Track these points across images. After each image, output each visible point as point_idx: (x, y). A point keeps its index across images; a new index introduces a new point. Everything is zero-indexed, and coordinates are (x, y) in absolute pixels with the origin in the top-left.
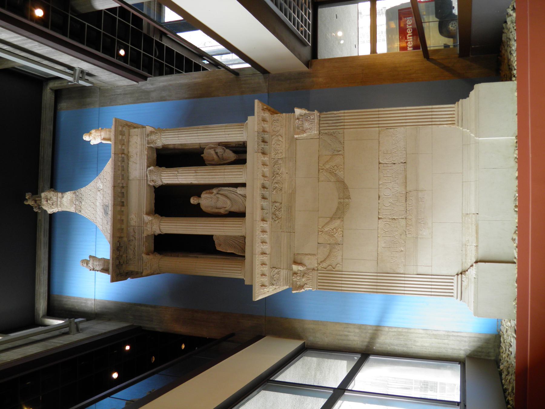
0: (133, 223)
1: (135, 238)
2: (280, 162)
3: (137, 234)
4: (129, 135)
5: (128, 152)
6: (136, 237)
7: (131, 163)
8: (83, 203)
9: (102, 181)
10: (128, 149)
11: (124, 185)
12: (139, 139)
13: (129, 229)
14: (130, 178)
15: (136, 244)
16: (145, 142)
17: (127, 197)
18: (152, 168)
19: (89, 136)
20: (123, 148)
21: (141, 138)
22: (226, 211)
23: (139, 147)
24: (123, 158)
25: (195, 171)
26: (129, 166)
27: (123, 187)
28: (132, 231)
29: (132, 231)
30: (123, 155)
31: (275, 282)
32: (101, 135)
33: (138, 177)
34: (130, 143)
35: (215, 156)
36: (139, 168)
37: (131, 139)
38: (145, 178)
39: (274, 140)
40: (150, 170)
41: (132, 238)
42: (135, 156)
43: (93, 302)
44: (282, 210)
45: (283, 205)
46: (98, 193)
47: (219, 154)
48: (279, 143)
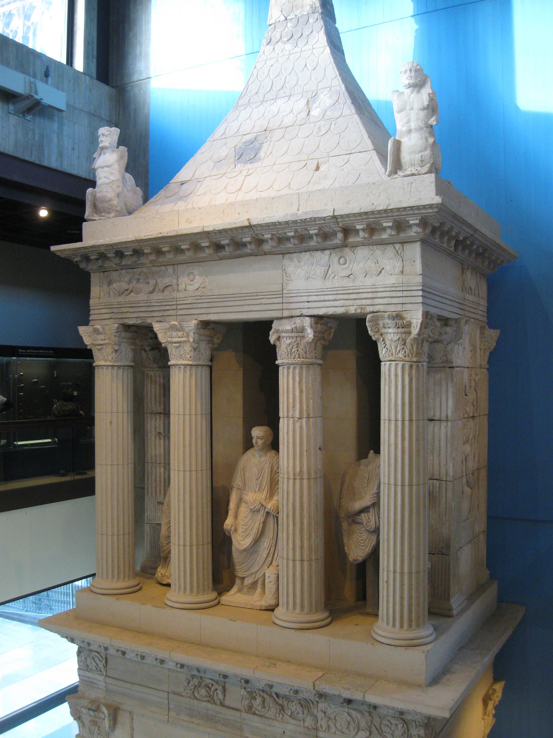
0: (184, 281)
1: (151, 292)
2: (309, 722)
3: (161, 296)
4: (403, 243)
5: (354, 246)
6: (156, 296)
7: (323, 257)
8: (288, 47)
9: (329, 113)
10: (363, 244)
11: (267, 247)
12: (392, 280)
13: (170, 269)
14: (286, 262)
15: (142, 297)
16: (380, 304)
17: (241, 256)
18: (310, 334)
19: (410, 86)
20: (362, 234)
21: (393, 288)
22: (229, 533)
23: (369, 281)
24: (335, 234)
25: (301, 471)
26: (318, 254)
27: (260, 242)
28: (167, 281)
29: (167, 281)
30: (340, 236)
31: (83, 658)
32: (410, 131)
33: (289, 288)
34: (378, 251)
35: (358, 505)
36: (312, 288)
37: (390, 251)
38: (286, 313)
39: (359, 716)
40: (302, 330)
41: (152, 282)
42: (346, 273)
43: (144, 76)
44: (209, 706)
45: (219, 708)
46: (303, 102)
47: (363, 516)
48: (351, 728)
